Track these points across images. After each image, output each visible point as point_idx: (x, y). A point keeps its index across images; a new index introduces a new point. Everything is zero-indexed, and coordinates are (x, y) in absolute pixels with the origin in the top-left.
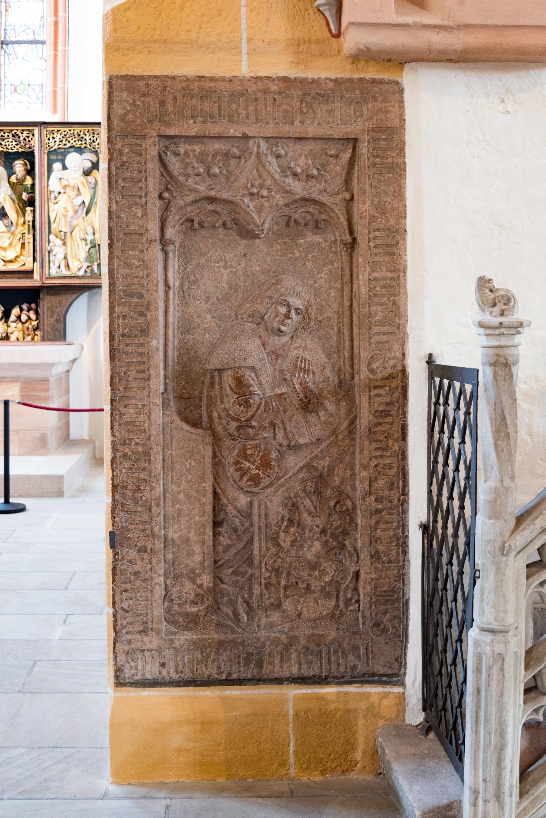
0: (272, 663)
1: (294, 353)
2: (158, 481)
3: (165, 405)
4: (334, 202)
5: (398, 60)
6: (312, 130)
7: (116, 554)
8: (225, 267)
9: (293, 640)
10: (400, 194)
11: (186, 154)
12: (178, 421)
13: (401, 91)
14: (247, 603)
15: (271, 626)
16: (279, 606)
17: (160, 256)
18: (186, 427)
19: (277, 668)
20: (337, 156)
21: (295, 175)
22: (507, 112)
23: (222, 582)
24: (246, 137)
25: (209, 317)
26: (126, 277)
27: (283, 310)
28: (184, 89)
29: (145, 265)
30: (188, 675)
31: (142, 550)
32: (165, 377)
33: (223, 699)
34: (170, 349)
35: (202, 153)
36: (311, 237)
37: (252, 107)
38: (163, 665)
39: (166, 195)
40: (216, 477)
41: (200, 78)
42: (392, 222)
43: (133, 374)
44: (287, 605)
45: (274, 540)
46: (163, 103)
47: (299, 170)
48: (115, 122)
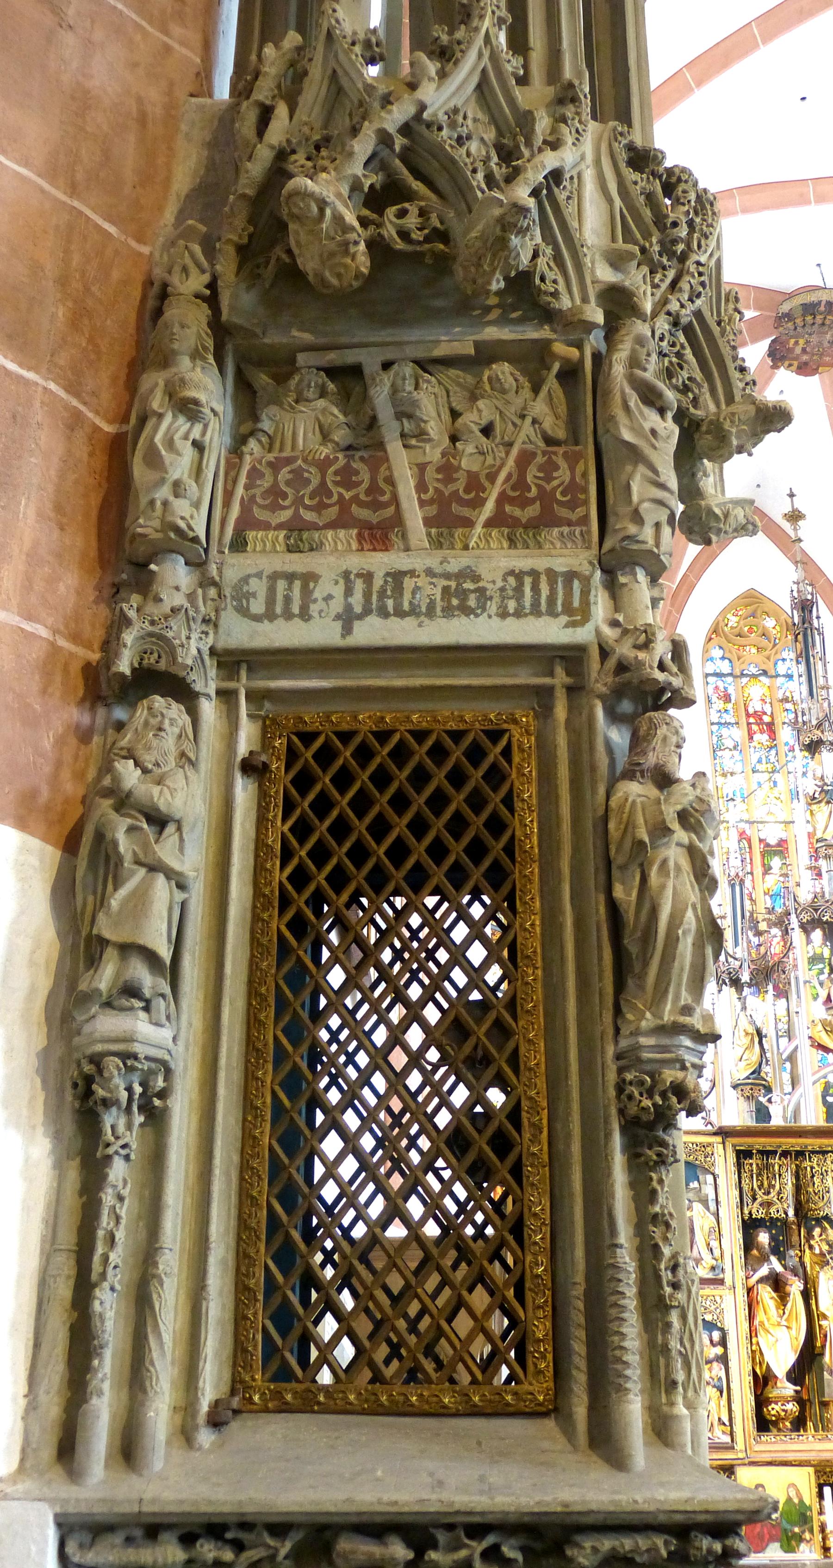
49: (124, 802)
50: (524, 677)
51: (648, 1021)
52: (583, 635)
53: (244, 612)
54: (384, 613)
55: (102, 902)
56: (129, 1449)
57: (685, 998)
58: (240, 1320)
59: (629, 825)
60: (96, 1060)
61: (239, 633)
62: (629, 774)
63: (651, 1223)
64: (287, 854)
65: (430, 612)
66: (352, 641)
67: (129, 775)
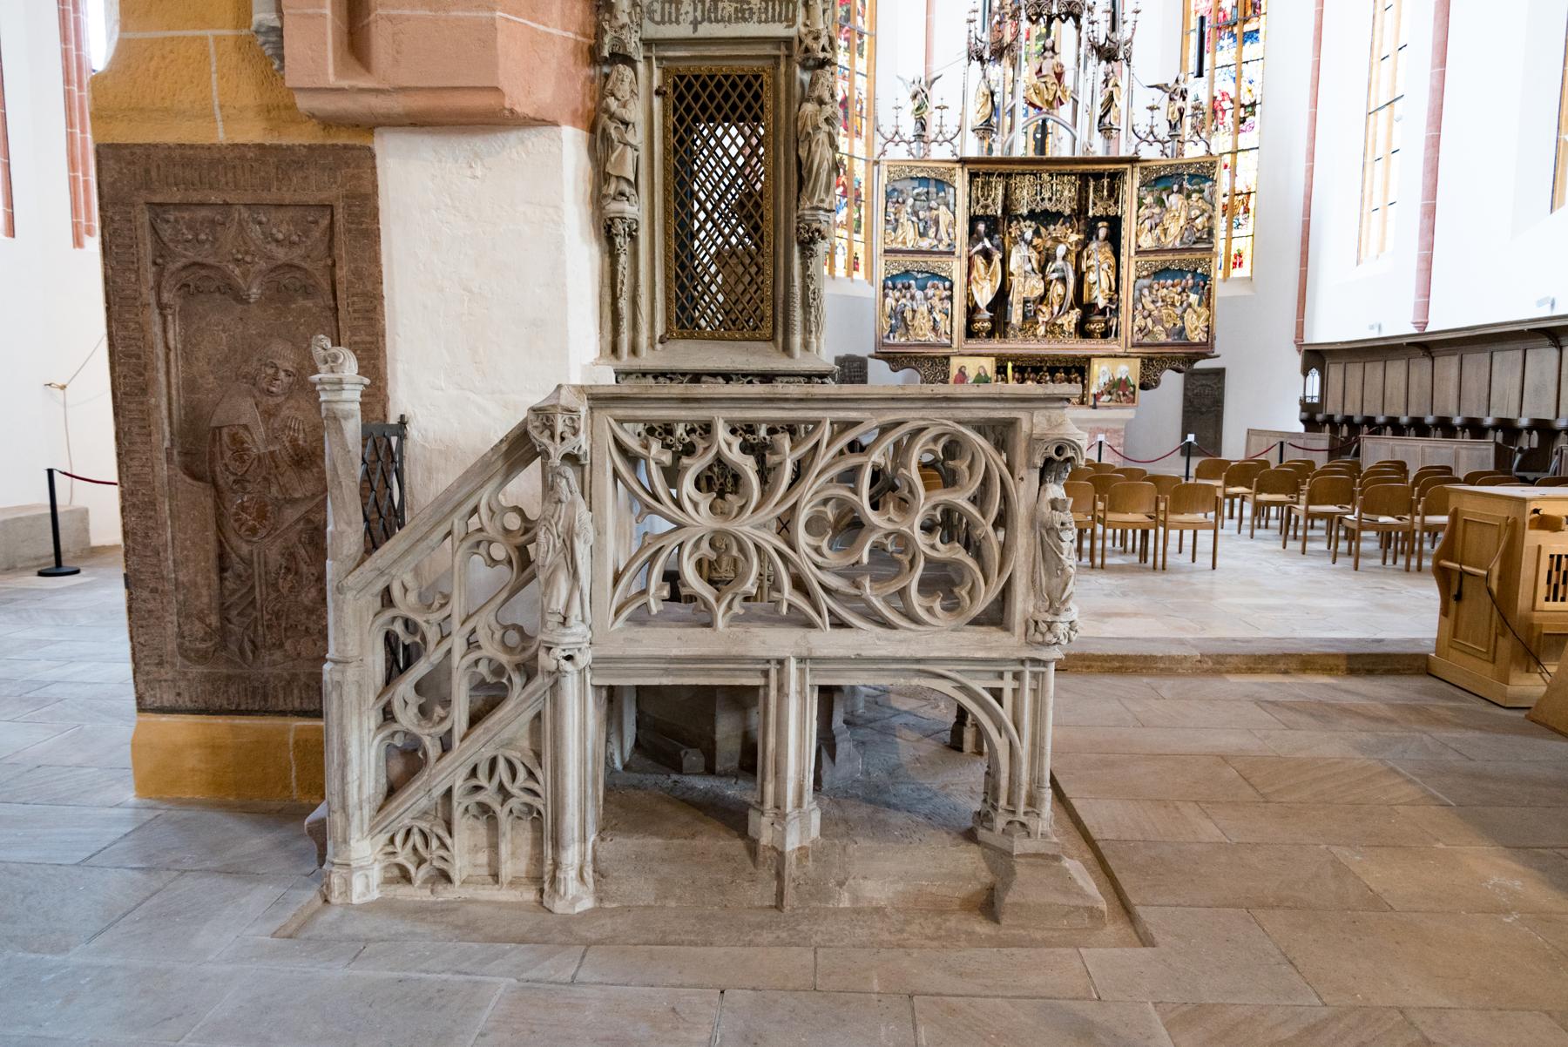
0: (276, 697)
1: (285, 412)
2: (165, 530)
3: (169, 459)
4: (317, 268)
5: (370, 125)
6: (288, 197)
7: (130, 594)
8: (224, 331)
9: (294, 677)
10: (376, 260)
11: (176, 221)
12: (181, 474)
13: (373, 157)
14: (253, 642)
15: (274, 664)
16: (281, 645)
17: (157, 318)
18: (188, 480)
19: (281, 702)
20: (316, 222)
21: (277, 241)
22: (474, 177)
23: (229, 621)
24: (227, 204)
25: (211, 378)
26: (124, 338)
27: (271, 371)
28: (166, 157)
29: (141, 328)
30: (202, 705)
31: (154, 591)
32: (172, 433)
33: (232, 727)
34: (175, 405)
35: (191, 220)
36: (301, 302)
37: (230, 175)
38: (179, 694)
39: (160, 261)
40: (220, 528)
41: (181, 146)
42: (369, 288)
43: (135, 430)
44: (288, 645)
45: (275, 586)
46: (147, 171)
47: (280, 236)
48: (105, 189)
49: (612, 116)
50: (768, 50)
51: (808, 205)
52: (792, 32)
53: (652, 20)
54: (710, 21)
55: (607, 159)
56: (634, 350)
57: (823, 196)
58: (667, 308)
59: (805, 125)
60: (612, 219)
61: (652, 31)
62: (808, 101)
63: (806, 276)
64: (676, 131)
65: (729, 21)
66: (697, 35)
67: (613, 104)
